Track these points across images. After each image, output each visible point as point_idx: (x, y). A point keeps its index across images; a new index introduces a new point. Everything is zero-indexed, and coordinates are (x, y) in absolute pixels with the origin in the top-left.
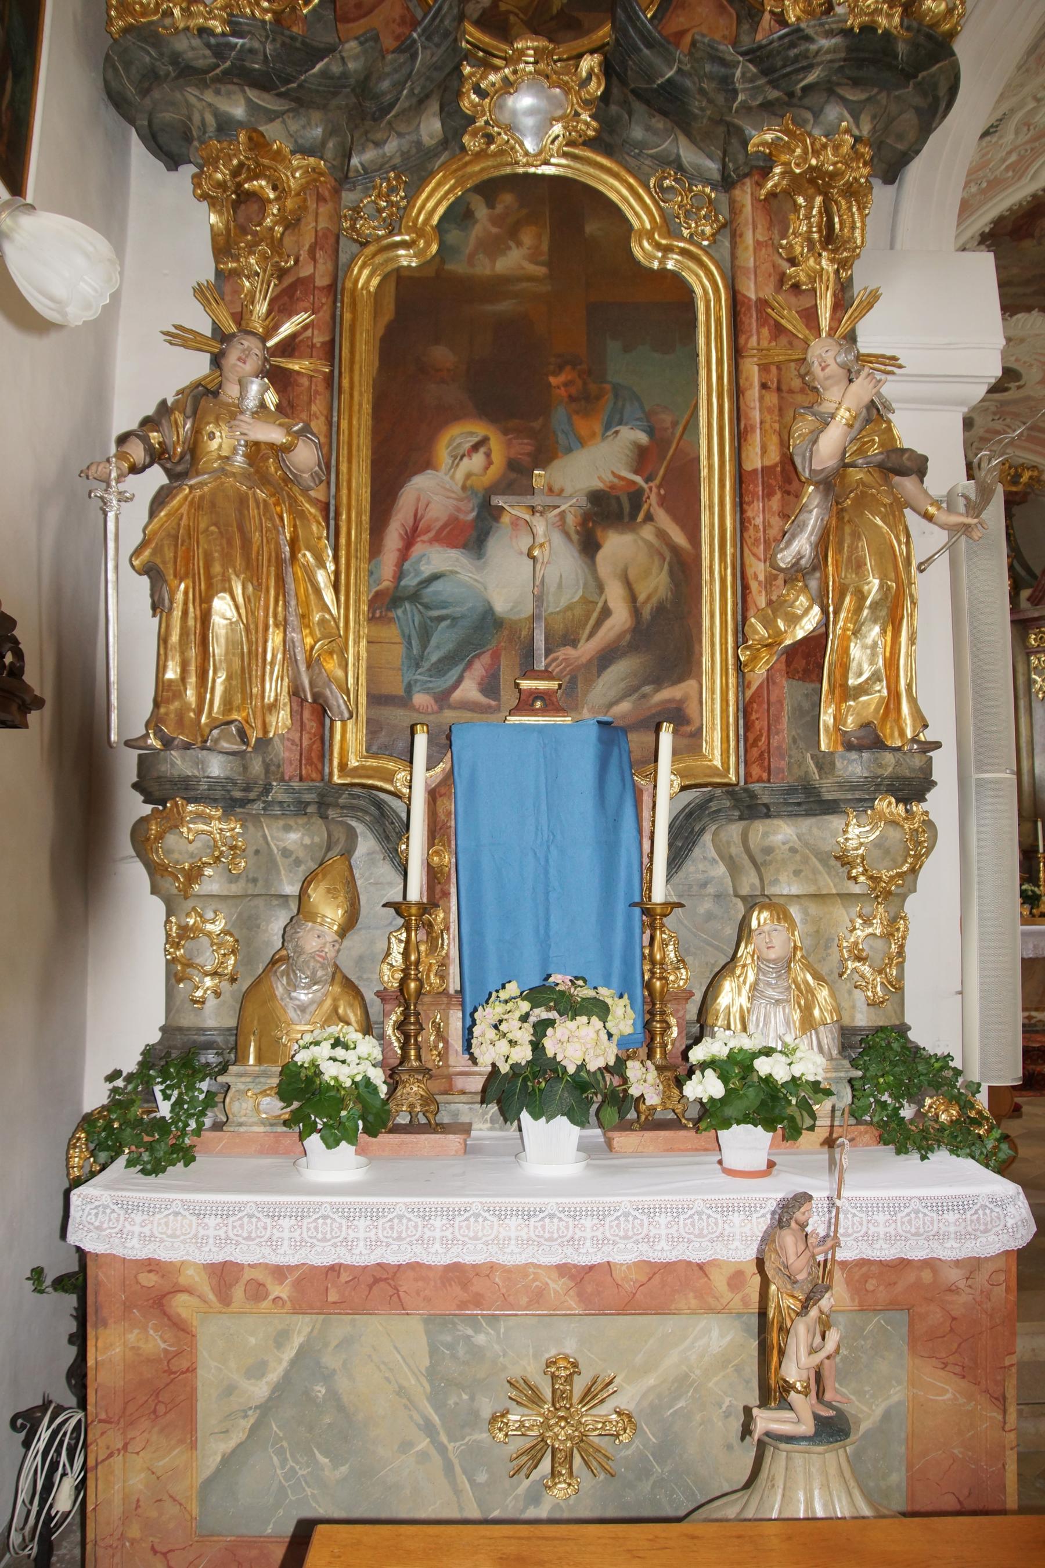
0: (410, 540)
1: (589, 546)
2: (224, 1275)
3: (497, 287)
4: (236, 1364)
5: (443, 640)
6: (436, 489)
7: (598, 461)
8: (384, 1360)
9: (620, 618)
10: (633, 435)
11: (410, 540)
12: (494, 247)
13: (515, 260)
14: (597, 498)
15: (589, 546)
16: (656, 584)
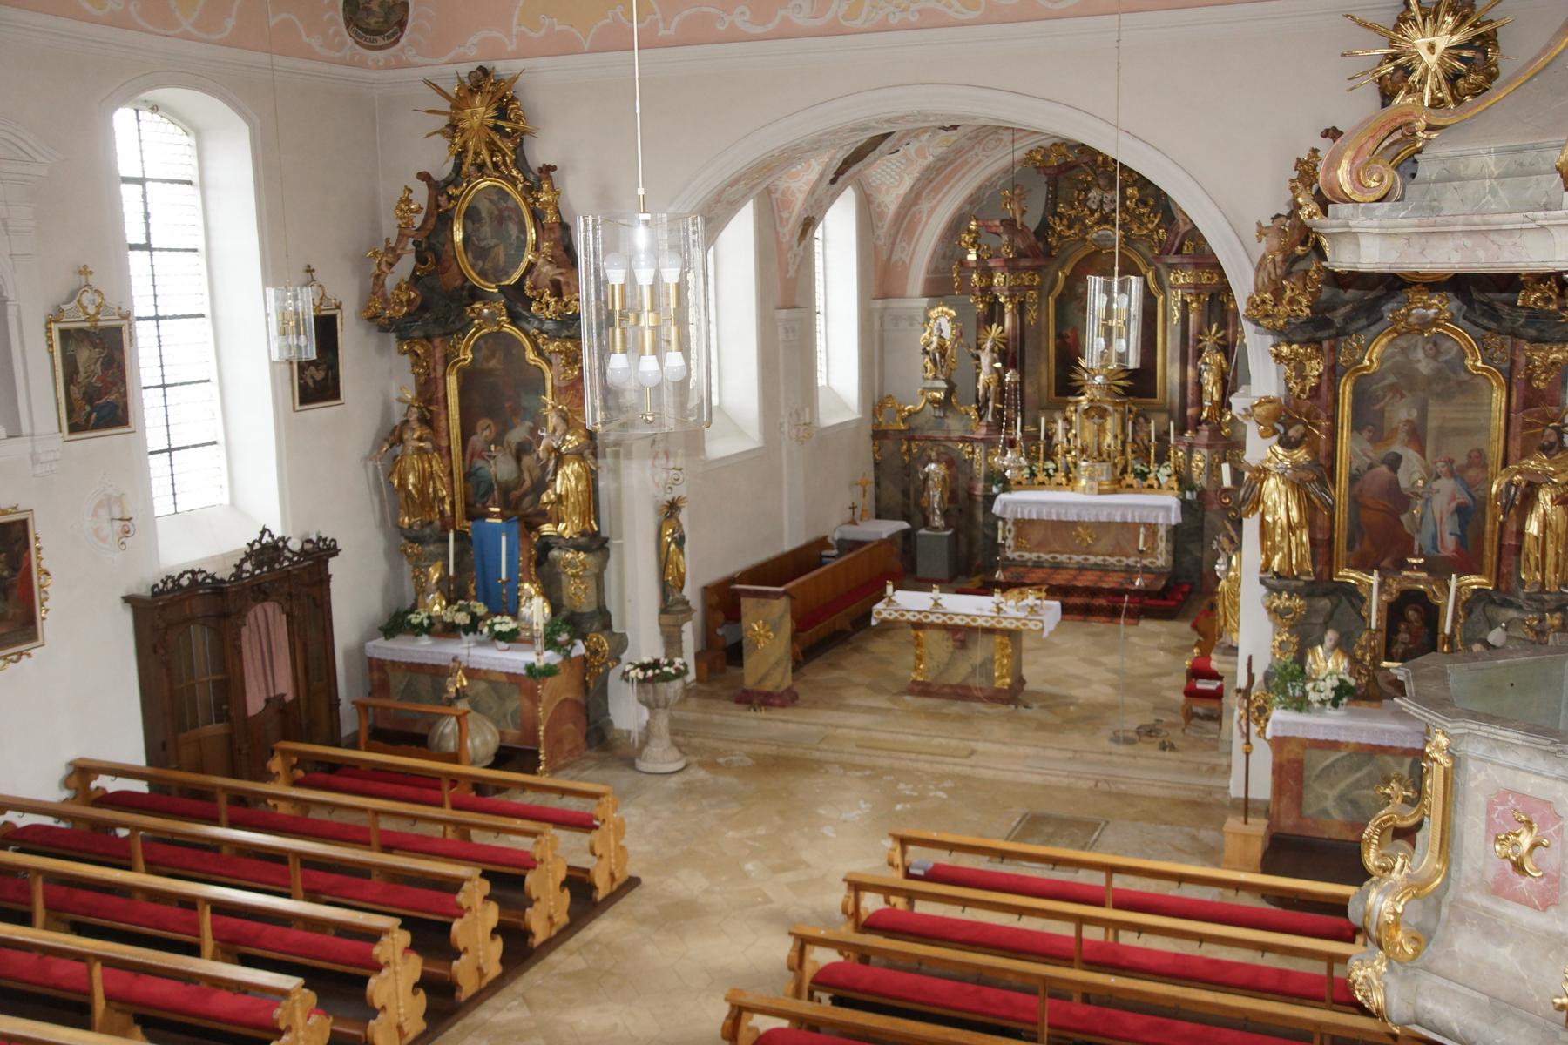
0: (472, 456)
1: (518, 460)
2: (393, 662)
3: (490, 372)
4: (398, 681)
5: (483, 488)
6: (477, 441)
7: (518, 434)
8: (424, 683)
9: (528, 483)
10: (529, 424)
11: (472, 456)
12: (488, 359)
13: (493, 364)
14: (519, 444)
15: (518, 460)
16: (537, 472)
